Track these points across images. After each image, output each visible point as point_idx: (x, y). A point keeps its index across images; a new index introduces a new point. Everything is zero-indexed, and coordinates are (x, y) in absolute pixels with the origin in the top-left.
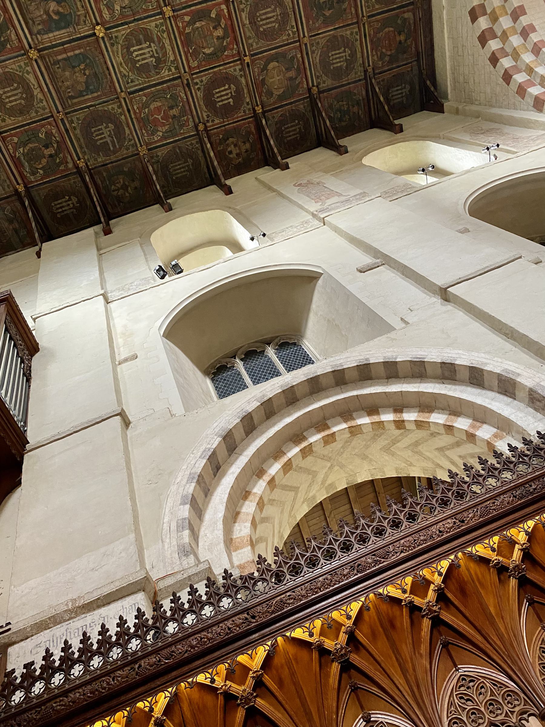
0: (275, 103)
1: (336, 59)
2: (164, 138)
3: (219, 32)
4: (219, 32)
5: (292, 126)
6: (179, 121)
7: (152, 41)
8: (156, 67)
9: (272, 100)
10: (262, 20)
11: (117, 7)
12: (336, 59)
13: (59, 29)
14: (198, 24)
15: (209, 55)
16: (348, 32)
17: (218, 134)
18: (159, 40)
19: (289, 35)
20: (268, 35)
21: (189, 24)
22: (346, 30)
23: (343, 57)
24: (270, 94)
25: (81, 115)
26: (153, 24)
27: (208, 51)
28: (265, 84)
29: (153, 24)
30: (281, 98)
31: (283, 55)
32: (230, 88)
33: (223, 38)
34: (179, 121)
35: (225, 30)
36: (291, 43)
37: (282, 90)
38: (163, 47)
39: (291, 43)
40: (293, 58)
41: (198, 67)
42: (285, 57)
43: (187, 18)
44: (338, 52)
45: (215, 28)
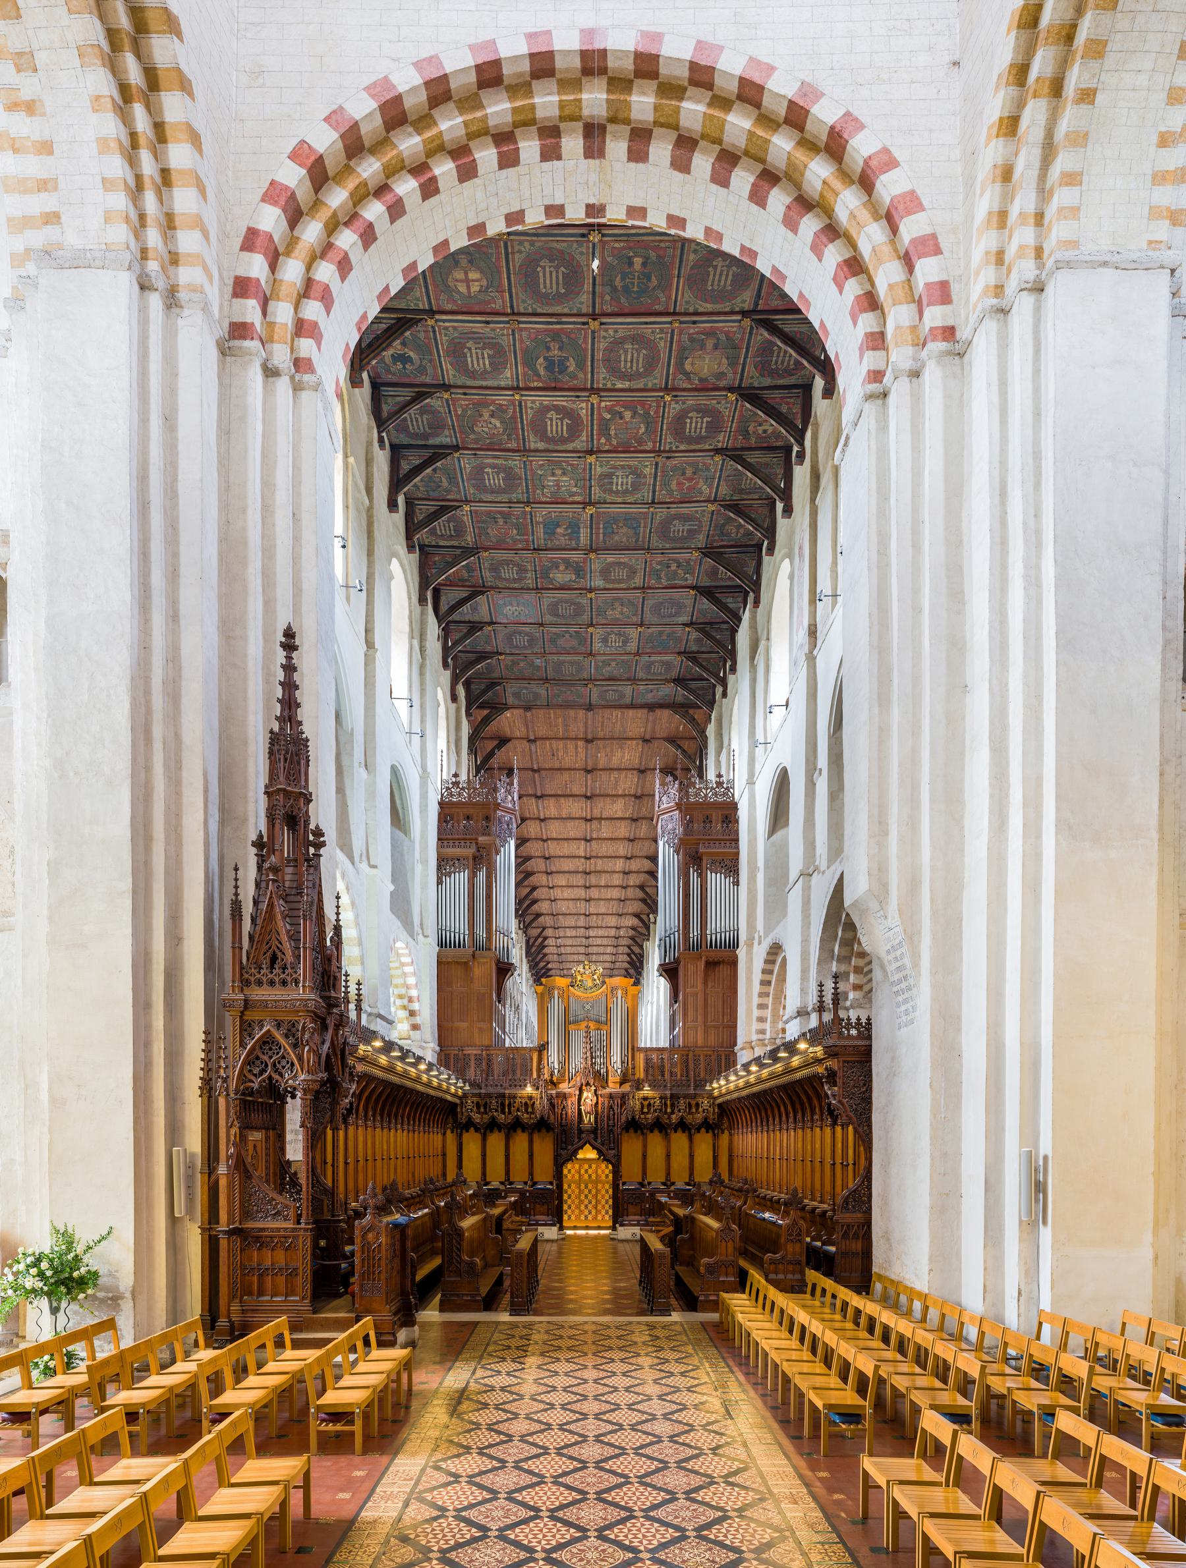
0: (735, 373)
1: (719, 281)
2: (710, 487)
3: (628, 415)
4: (628, 415)
5: (778, 356)
6: (701, 470)
7: (613, 474)
8: (639, 476)
9: (730, 375)
10: (631, 367)
11: (575, 489)
12: (719, 281)
13: (579, 533)
14: (612, 432)
15: (647, 428)
16: (692, 257)
17: (736, 439)
18: (614, 467)
19: (661, 338)
20: (651, 364)
21: (608, 440)
22: (687, 260)
23: (722, 271)
24: (721, 376)
25: (654, 538)
26: (599, 469)
27: (643, 430)
28: (706, 379)
29: (599, 469)
30: (733, 363)
31: (682, 349)
32: (691, 418)
33: (635, 413)
34: (701, 470)
35: (626, 408)
36: (672, 338)
37: (725, 361)
38: (623, 467)
39: (672, 338)
40: (692, 340)
41: (654, 442)
42: (685, 349)
43: (603, 440)
44: (711, 277)
45: (621, 418)
